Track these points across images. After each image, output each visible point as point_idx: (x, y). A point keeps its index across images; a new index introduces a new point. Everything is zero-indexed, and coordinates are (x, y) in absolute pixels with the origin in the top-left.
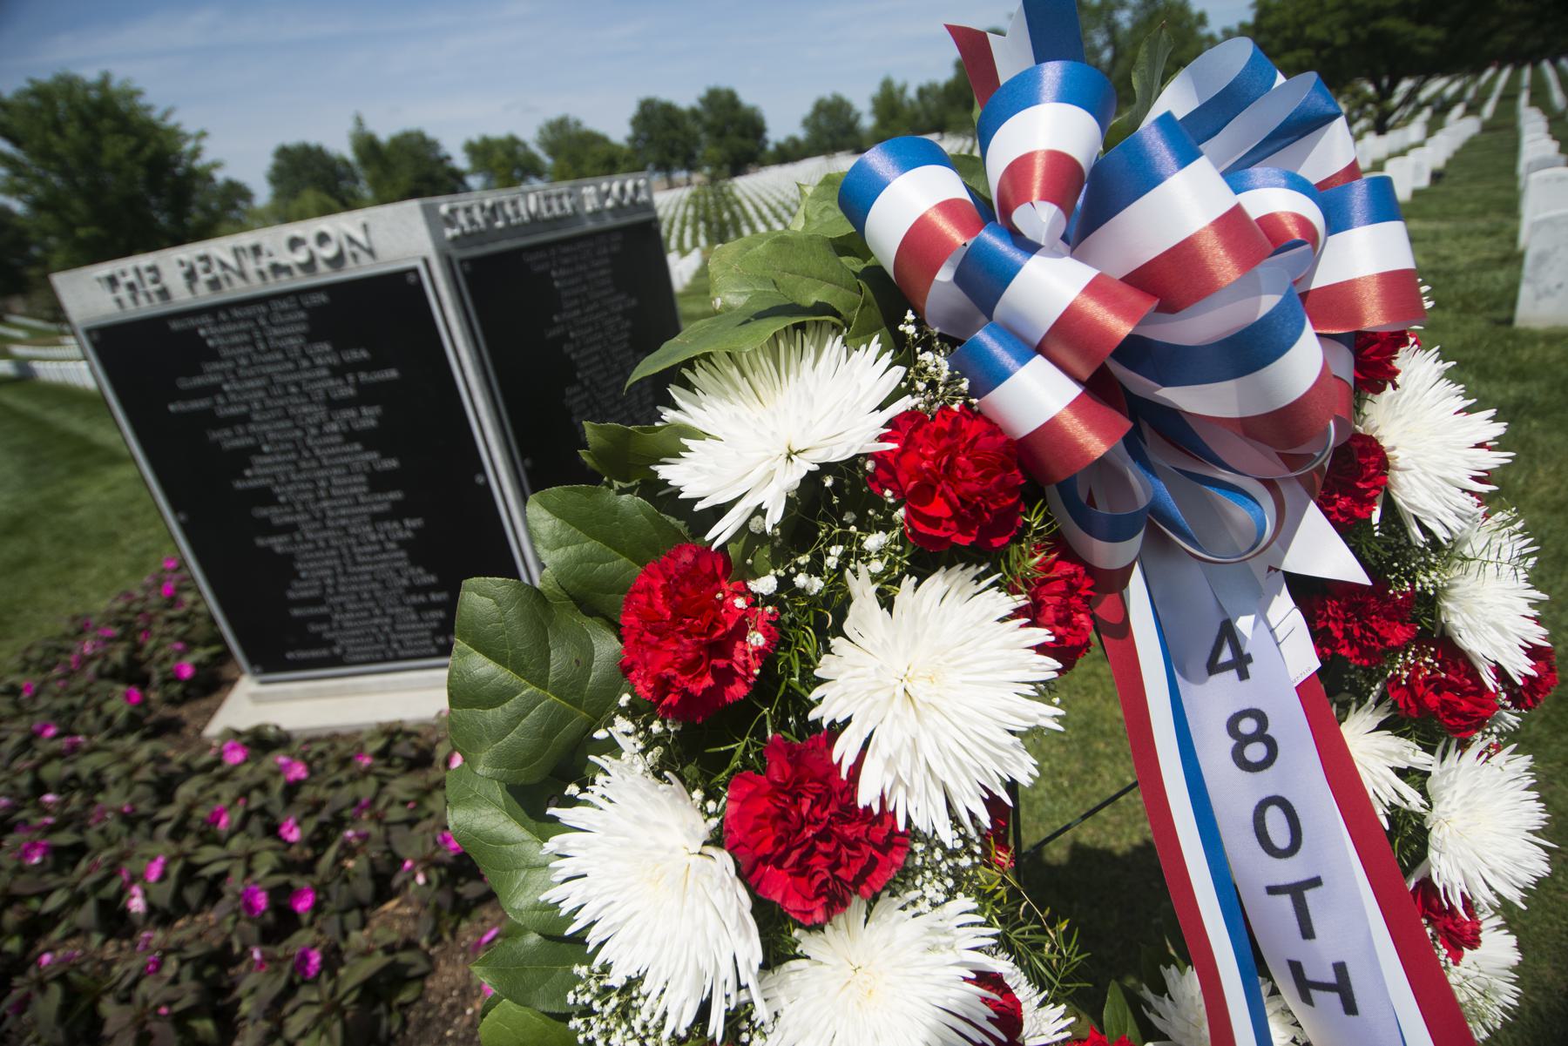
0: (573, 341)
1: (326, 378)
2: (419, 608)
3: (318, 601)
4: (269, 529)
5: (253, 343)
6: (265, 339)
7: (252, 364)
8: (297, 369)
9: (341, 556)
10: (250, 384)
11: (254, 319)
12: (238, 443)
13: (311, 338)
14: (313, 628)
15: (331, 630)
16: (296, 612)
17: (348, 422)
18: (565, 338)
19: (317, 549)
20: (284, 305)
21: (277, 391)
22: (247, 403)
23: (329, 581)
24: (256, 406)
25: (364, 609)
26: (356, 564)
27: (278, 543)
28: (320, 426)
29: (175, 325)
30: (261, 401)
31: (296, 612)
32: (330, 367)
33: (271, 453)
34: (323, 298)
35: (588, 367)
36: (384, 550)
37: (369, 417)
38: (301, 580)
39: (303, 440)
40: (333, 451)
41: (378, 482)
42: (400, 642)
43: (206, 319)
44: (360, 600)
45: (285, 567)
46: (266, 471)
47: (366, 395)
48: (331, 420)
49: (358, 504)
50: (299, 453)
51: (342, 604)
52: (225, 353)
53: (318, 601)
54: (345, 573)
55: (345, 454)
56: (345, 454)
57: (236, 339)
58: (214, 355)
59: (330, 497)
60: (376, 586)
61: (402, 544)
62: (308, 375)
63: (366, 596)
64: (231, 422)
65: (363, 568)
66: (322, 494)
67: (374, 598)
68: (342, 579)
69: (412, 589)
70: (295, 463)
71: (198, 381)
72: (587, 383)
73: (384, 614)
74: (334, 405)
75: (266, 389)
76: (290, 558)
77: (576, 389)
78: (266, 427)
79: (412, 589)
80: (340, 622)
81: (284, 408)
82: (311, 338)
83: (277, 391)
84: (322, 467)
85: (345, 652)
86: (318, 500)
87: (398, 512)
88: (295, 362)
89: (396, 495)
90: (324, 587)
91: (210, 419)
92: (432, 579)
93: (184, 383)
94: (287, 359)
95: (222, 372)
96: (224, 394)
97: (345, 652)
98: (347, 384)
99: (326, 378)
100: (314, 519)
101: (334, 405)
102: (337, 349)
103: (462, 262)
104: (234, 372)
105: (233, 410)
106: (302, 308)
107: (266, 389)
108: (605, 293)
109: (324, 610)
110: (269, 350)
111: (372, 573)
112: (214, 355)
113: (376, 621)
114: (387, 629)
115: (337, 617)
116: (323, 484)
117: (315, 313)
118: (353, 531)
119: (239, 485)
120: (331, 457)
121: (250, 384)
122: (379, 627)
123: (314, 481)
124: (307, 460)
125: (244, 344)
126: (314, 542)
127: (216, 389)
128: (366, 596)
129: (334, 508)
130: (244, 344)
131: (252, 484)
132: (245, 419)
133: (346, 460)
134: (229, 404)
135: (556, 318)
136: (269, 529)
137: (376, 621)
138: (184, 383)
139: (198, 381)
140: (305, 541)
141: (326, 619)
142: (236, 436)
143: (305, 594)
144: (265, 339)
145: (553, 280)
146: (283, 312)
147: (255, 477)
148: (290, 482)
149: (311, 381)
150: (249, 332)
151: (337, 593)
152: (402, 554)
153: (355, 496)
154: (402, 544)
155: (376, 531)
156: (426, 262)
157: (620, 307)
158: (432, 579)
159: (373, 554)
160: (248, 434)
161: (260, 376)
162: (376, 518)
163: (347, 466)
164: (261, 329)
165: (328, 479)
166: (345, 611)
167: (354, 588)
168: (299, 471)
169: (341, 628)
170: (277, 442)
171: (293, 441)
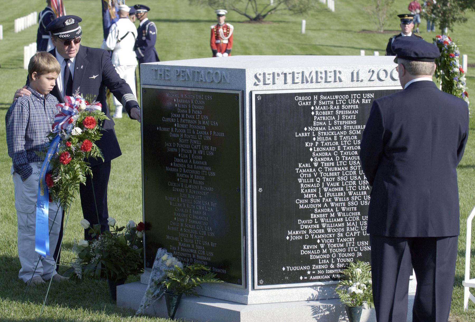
1: (204, 130)
6: (191, 109)
7: (185, 118)
8: (197, 125)
10: (182, 126)
12: (172, 150)
17: (205, 151)
23: (182, 225)
25: (189, 243)
26: (192, 219)
28: (197, 150)
30: (184, 134)
31: (168, 237)
33: (180, 158)
34: (210, 97)
35: (320, 157)
39: (191, 154)
40: (198, 163)
46: (177, 165)
50: (188, 161)
51: (183, 238)
55: (201, 165)
56: (201, 165)
59: (192, 184)
62: (199, 127)
63: (191, 236)
65: (194, 222)
71: (168, 120)
72: (316, 165)
73: (195, 249)
75: (186, 129)
78: (182, 146)
80: (180, 247)
81: (189, 139)
84: (193, 169)
86: (188, 184)
88: (197, 120)
94: (195, 119)
95: (176, 118)
96: (174, 127)
98: (209, 135)
99: (204, 130)
101: (204, 142)
103: (256, 95)
105: (174, 135)
107: (186, 129)
108: (349, 122)
109: (176, 239)
110: (191, 114)
111: (196, 225)
113: (192, 251)
115: (180, 244)
116: (192, 176)
120: (197, 165)
121: (182, 126)
122: (192, 254)
124: (190, 164)
125: (185, 109)
128: (191, 236)
129: (192, 189)
130: (185, 109)
131: (171, 169)
132: (176, 140)
133: (201, 168)
134: (174, 133)
135: (306, 129)
137: (192, 251)
142: (172, 147)
144: (191, 109)
145: (311, 111)
147: (173, 167)
150: (187, 105)
153: (200, 185)
160: (176, 147)
161: (185, 124)
165: (194, 174)
166: (183, 242)
168: (186, 169)
170: (184, 153)
171: (188, 154)
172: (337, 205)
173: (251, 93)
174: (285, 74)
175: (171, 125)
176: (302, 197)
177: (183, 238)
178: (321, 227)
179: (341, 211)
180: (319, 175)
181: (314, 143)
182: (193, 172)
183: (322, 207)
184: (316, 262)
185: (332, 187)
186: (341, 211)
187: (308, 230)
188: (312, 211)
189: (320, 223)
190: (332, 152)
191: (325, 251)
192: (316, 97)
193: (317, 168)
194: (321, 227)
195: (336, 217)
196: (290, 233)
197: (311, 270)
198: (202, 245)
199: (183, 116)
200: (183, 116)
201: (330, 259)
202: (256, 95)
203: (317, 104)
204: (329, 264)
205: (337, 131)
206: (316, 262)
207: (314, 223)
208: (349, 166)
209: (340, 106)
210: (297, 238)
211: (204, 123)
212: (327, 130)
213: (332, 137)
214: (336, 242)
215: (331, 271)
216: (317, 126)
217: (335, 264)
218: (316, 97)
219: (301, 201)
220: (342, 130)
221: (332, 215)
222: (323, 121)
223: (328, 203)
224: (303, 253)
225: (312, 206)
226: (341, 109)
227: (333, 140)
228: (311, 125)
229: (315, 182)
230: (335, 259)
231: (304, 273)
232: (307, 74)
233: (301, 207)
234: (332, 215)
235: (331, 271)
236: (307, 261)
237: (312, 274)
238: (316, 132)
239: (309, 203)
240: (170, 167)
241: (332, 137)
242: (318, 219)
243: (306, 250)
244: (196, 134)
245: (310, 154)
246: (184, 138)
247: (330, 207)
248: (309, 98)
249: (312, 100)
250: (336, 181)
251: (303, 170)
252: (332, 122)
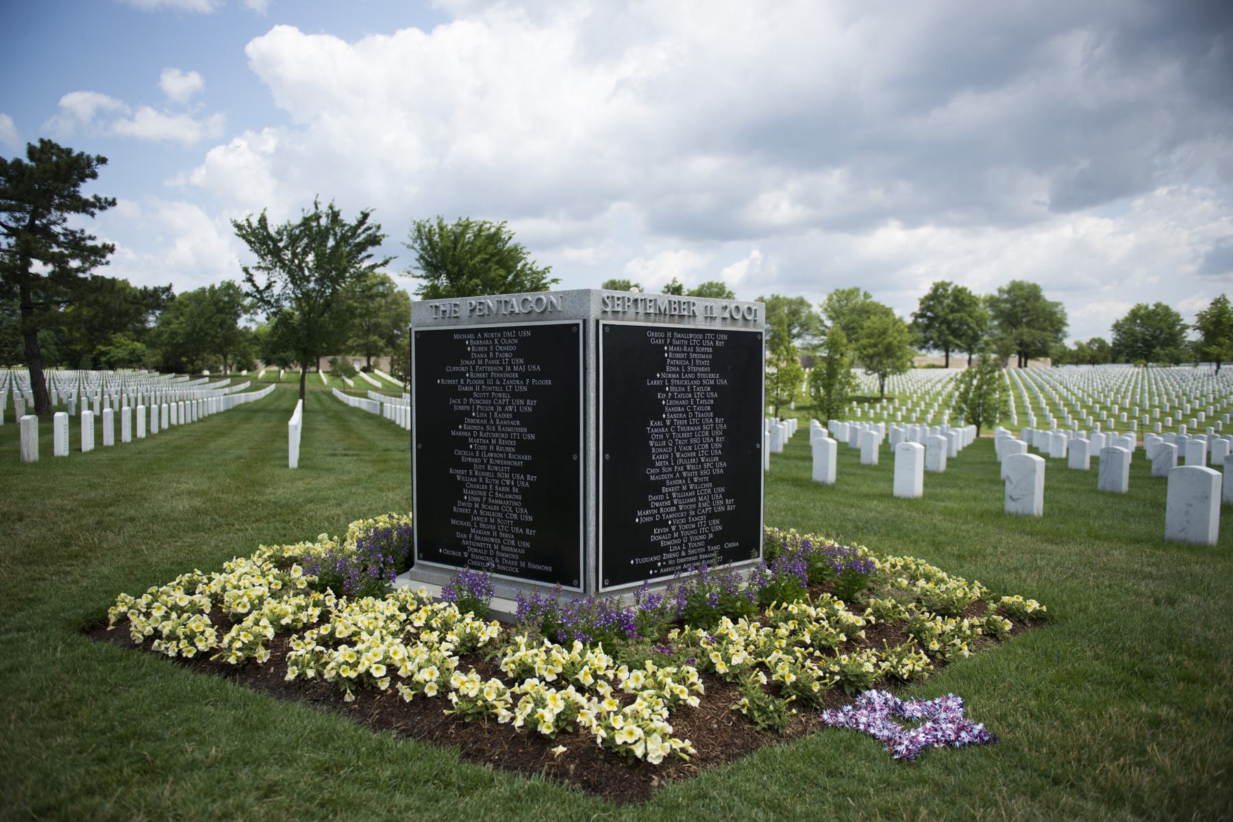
0: (667, 393)
2: (518, 537)
3: (466, 517)
5: (488, 353)
6: (494, 352)
9: (488, 490)
11: (493, 340)
12: (462, 408)
13: (516, 354)
15: (467, 539)
16: (453, 522)
18: (661, 389)
19: (478, 483)
20: (509, 334)
21: (490, 382)
22: (474, 386)
23: (477, 506)
24: (478, 388)
26: (494, 498)
27: (459, 474)
28: (503, 407)
29: (456, 337)
31: (453, 522)
32: (520, 373)
36: (511, 493)
37: (529, 406)
38: (463, 500)
41: (522, 447)
42: (500, 558)
43: (471, 336)
44: (489, 523)
45: (458, 488)
47: (533, 392)
48: (510, 404)
49: (507, 459)
51: (478, 523)
52: (474, 355)
53: (466, 517)
54: (487, 502)
57: (481, 349)
58: (467, 356)
59: (495, 451)
60: (499, 515)
61: (522, 491)
63: (492, 521)
66: (492, 448)
67: (496, 524)
68: (483, 506)
69: (518, 523)
70: (484, 426)
71: (456, 369)
74: (514, 395)
75: (485, 380)
76: (462, 484)
77: (659, 423)
79: (518, 523)
81: (490, 392)
82: (516, 354)
83: (490, 382)
84: (497, 431)
85: (469, 556)
86: (488, 451)
87: (526, 469)
89: (527, 458)
90: (473, 509)
91: (453, 392)
92: (531, 518)
93: (449, 369)
96: (465, 378)
97: (469, 556)
100: (482, 463)
101: (514, 395)
102: (526, 364)
103: (604, 325)
104: (474, 367)
106: (517, 337)
107: (485, 380)
108: (702, 369)
109: (468, 524)
110: (494, 358)
112: (467, 356)
114: (496, 547)
115: (473, 531)
116: (494, 442)
117: (523, 340)
118: (499, 475)
119: (453, 433)
122: (492, 544)
123: (490, 439)
126: (478, 477)
127: (462, 375)
128: (492, 521)
132: (469, 395)
133: (510, 430)
134: (465, 385)
138: (449, 369)
139: (456, 369)
140: (473, 476)
141: (466, 530)
143: (461, 510)
144: (494, 352)
146: (507, 338)
147: (462, 430)
148: (478, 437)
149: (508, 379)
150: (488, 346)
151: (478, 515)
152: (520, 497)
154: (522, 491)
155: (511, 479)
156: (584, 321)
157: (712, 382)
158: (531, 518)
159: (505, 493)
160: (468, 404)
162: (514, 470)
163: (509, 433)
164: (494, 346)
166: (478, 528)
167: (488, 514)
168: (485, 431)
169: (473, 539)
170: (480, 411)
171: (488, 413)
172: (690, 474)
173: (597, 322)
174: (636, 300)
175: (461, 375)
176: (653, 466)
177: (478, 523)
178: (672, 504)
179: (693, 482)
180: (671, 437)
181: (667, 393)
182: (497, 435)
183: (674, 479)
184: (666, 550)
185: (683, 452)
186: (693, 482)
187: (658, 508)
188: (663, 483)
189: (671, 499)
190: (685, 406)
191: (676, 535)
192: (669, 334)
193: (669, 427)
194: (672, 504)
195: (689, 490)
196: (639, 513)
197: (662, 561)
198: (510, 532)
199: (480, 362)
200: (480, 362)
201: (681, 545)
202: (604, 325)
203: (671, 344)
204: (680, 551)
205: (690, 379)
206: (666, 550)
207: (665, 500)
208: (701, 425)
209: (694, 347)
210: (647, 519)
211: (515, 368)
212: (680, 379)
213: (686, 387)
214: (687, 523)
215: (682, 560)
216: (670, 373)
217: (686, 551)
218: (669, 334)
219: (652, 471)
220: (696, 379)
221: (684, 488)
222: (676, 366)
223: (680, 473)
224: (653, 538)
225: (664, 477)
226: (694, 352)
227: (686, 392)
228: (664, 370)
229: (667, 446)
230: (687, 545)
231: (653, 565)
232: (659, 302)
233: (652, 478)
234: (684, 488)
235: (682, 560)
236: (658, 549)
237: (662, 566)
238: (669, 380)
239: (661, 473)
240: (458, 430)
241: (686, 387)
242: (670, 494)
243: (657, 535)
244: (501, 385)
245: (662, 409)
246: (481, 391)
247: (682, 477)
248: (662, 335)
249: (665, 338)
250: (689, 444)
251: (655, 429)
252: (686, 367)
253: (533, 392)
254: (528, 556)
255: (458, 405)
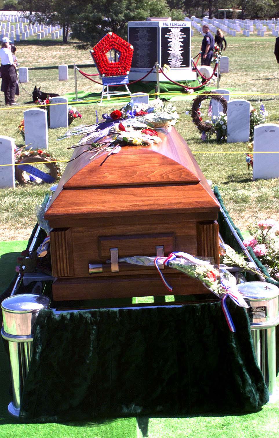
2: (180, 61)
3: (171, 59)
4: (169, 50)
13: (180, 32)
14: (169, 63)
37: (182, 40)
45: (169, 55)
47: (183, 38)
53: (171, 59)
58: (171, 32)
64: (170, 38)
69: (180, 59)
76: (170, 54)
79: (180, 59)
91: (168, 38)
93: (168, 34)
112: (171, 32)
136: (169, 50)
253: (183, 38)
254: (182, 64)
255: (169, 40)
